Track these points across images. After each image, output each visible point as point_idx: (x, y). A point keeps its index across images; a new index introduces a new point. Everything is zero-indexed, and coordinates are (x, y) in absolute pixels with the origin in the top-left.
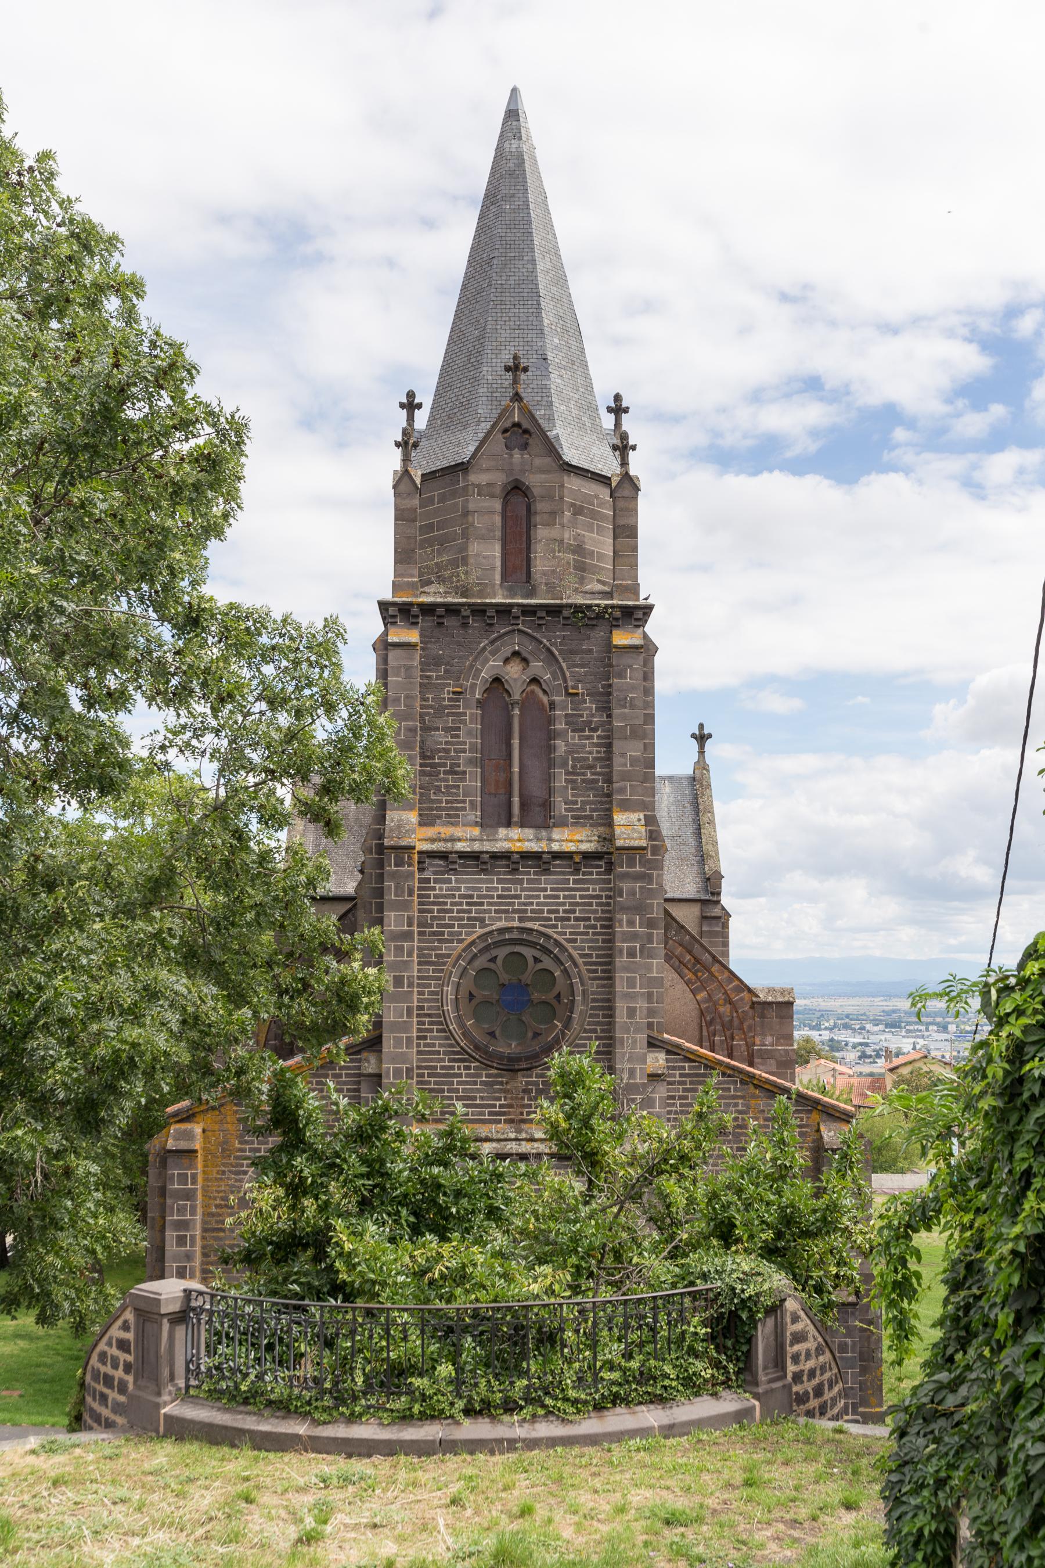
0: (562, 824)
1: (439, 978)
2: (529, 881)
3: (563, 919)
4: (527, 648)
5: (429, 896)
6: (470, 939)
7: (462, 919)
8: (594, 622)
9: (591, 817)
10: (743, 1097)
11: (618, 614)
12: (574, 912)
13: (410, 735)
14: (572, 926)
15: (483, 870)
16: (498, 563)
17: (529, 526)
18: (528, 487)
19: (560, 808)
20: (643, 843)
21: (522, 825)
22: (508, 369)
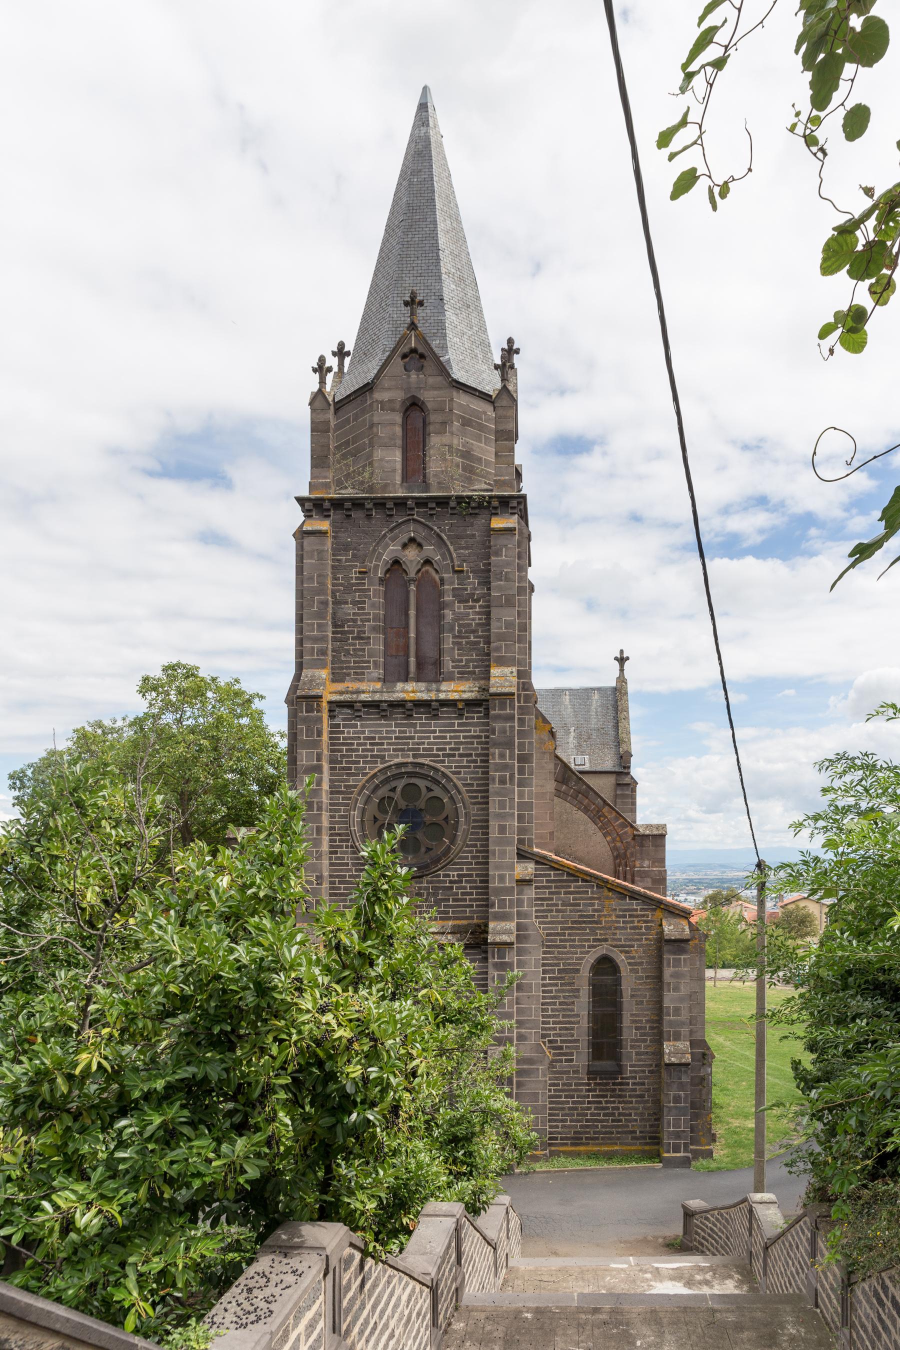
0: (450, 678)
1: (347, 805)
2: (421, 725)
3: (449, 755)
4: (420, 534)
5: (339, 739)
6: (373, 772)
7: (366, 756)
8: (477, 511)
9: (474, 673)
10: (598, 899)
11: (495, 503)
12: (459, 749)
13: (322, 607)
14: (457, 761)
15: (383, 716)
16: (399, 466)
17: (425, 435)
18: (423, 402)
19: (448, 665)
20: (514, 690)
21: (418, 680)
22: (406, 304)
